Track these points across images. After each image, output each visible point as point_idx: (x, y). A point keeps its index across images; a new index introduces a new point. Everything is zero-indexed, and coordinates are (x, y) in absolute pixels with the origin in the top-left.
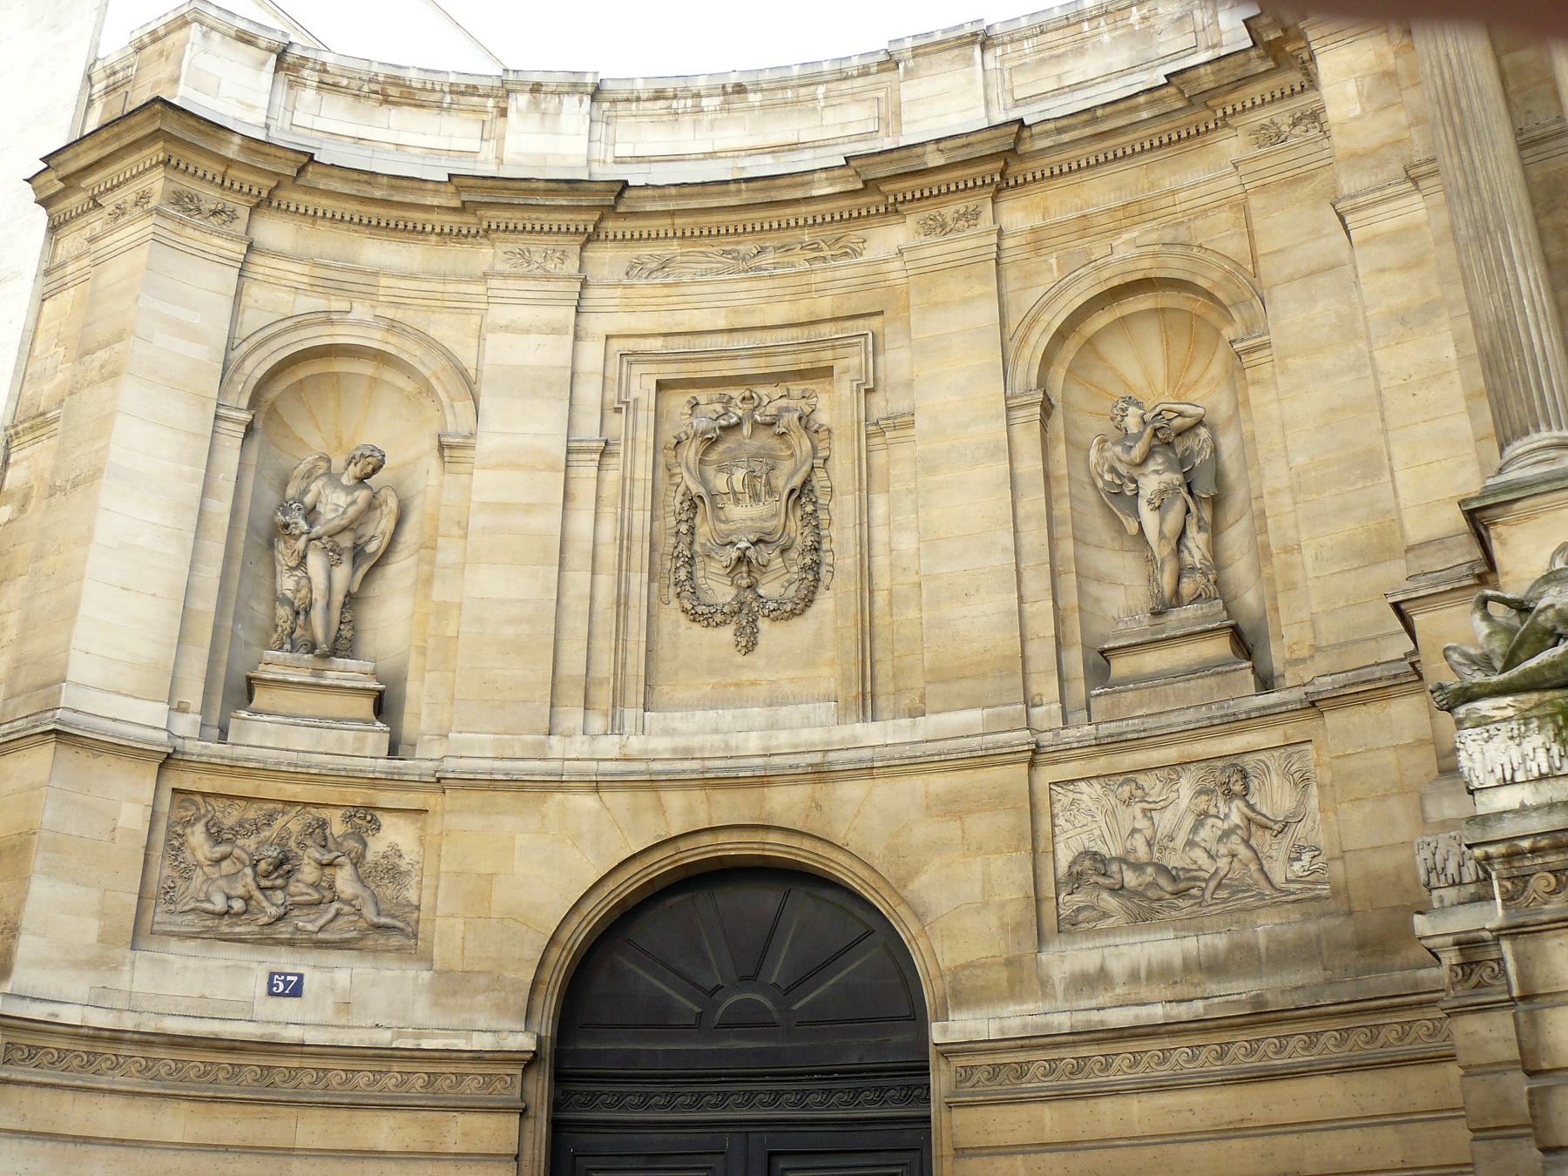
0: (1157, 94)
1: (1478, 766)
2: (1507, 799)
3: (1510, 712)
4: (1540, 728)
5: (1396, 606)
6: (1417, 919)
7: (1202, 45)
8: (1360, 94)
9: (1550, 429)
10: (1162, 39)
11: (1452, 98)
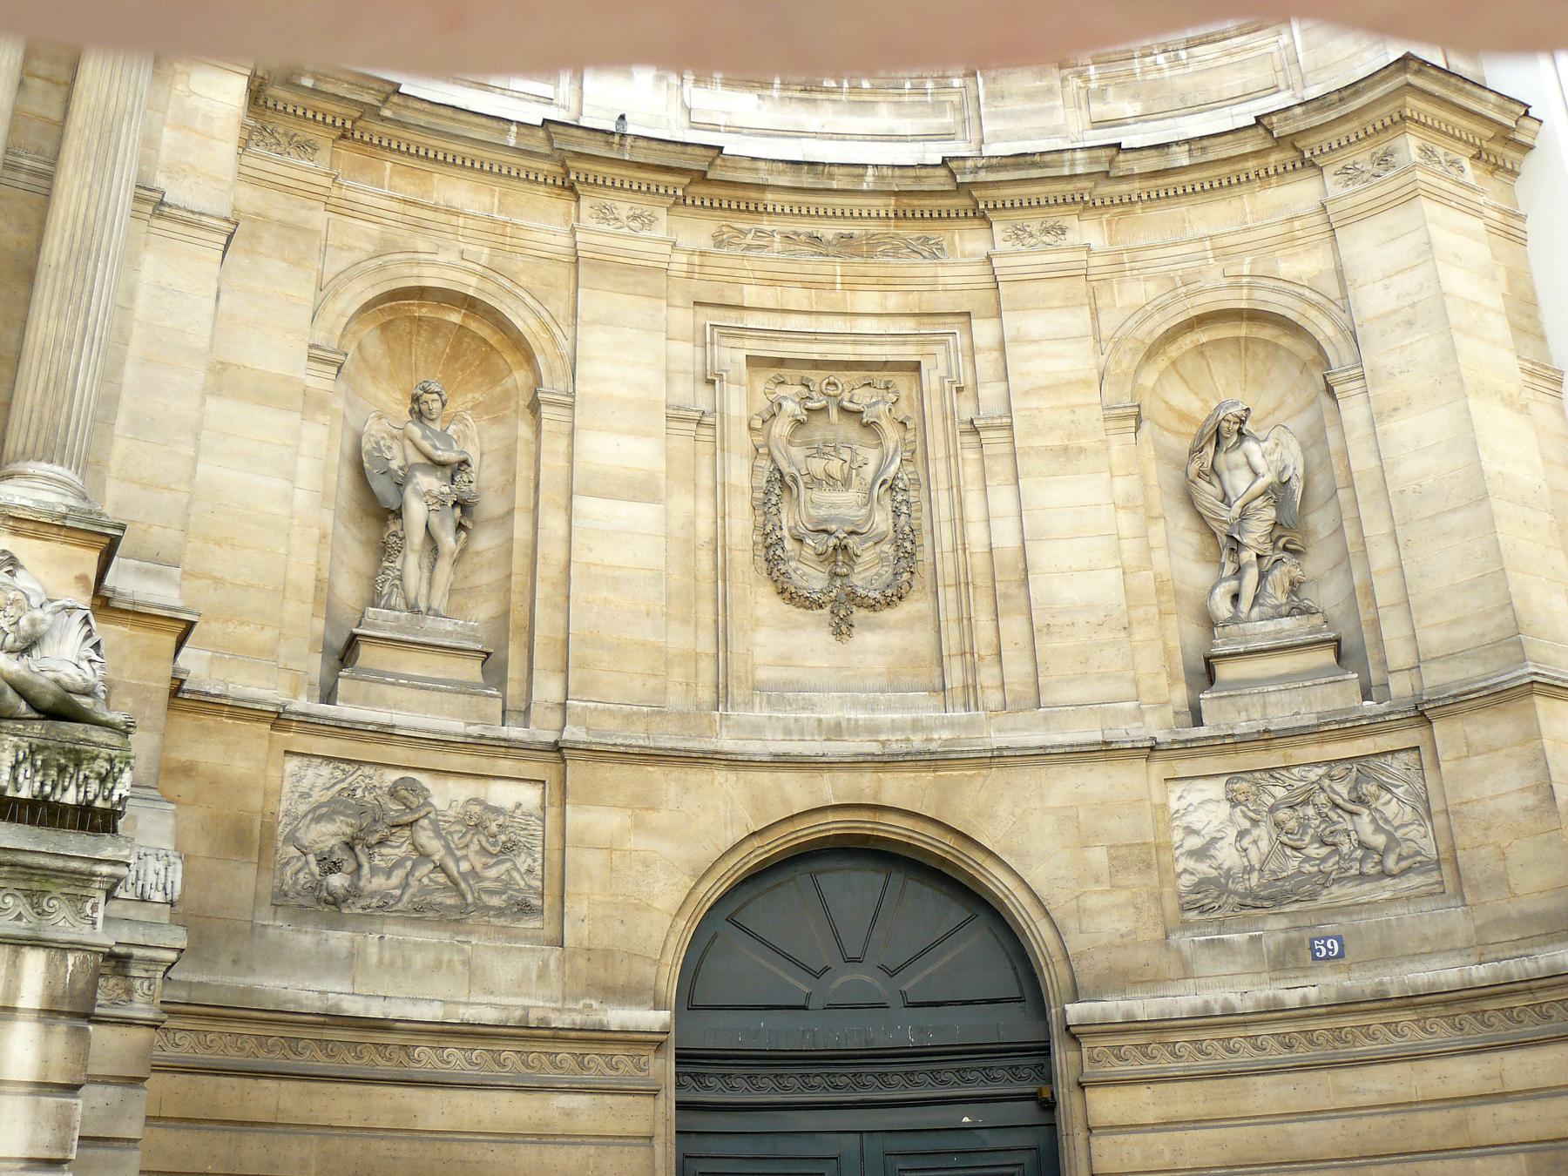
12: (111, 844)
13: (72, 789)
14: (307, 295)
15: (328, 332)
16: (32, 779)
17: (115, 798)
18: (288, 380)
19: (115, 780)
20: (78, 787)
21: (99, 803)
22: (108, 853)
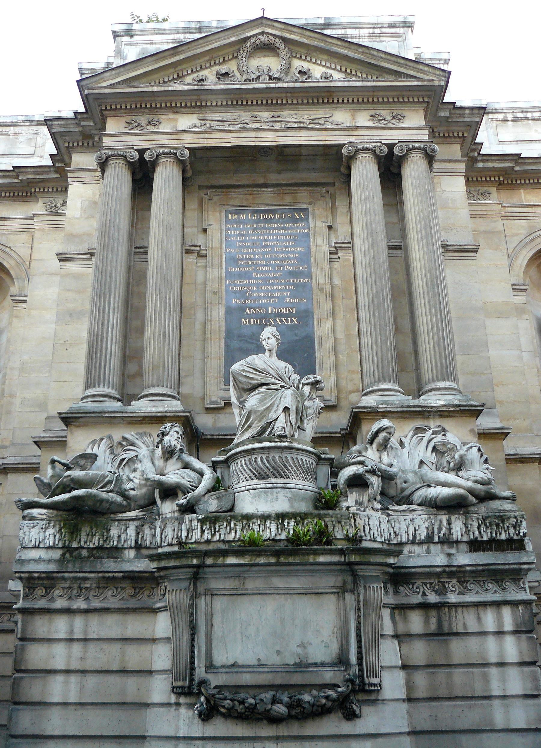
0: (8, 174)
1: (26, 538)
2: (34, 554)
3: (44, 517)
4: (54, 526)
5: (35, 442)
6: (10, 582)
7: (36, 154)
8: (82, 208)
9: (104, 387)
10: (20, 145)
11: (107, 230)
12: (526, 555)
13: (503, 533)
14: (505, 262)
15: (518, 277)
16: (486, 532)
17: (521, 534)
18: (507, 303)
19: (520, 526)
20: (505, 531)
21: (515, 537)
22: (525, 559)
